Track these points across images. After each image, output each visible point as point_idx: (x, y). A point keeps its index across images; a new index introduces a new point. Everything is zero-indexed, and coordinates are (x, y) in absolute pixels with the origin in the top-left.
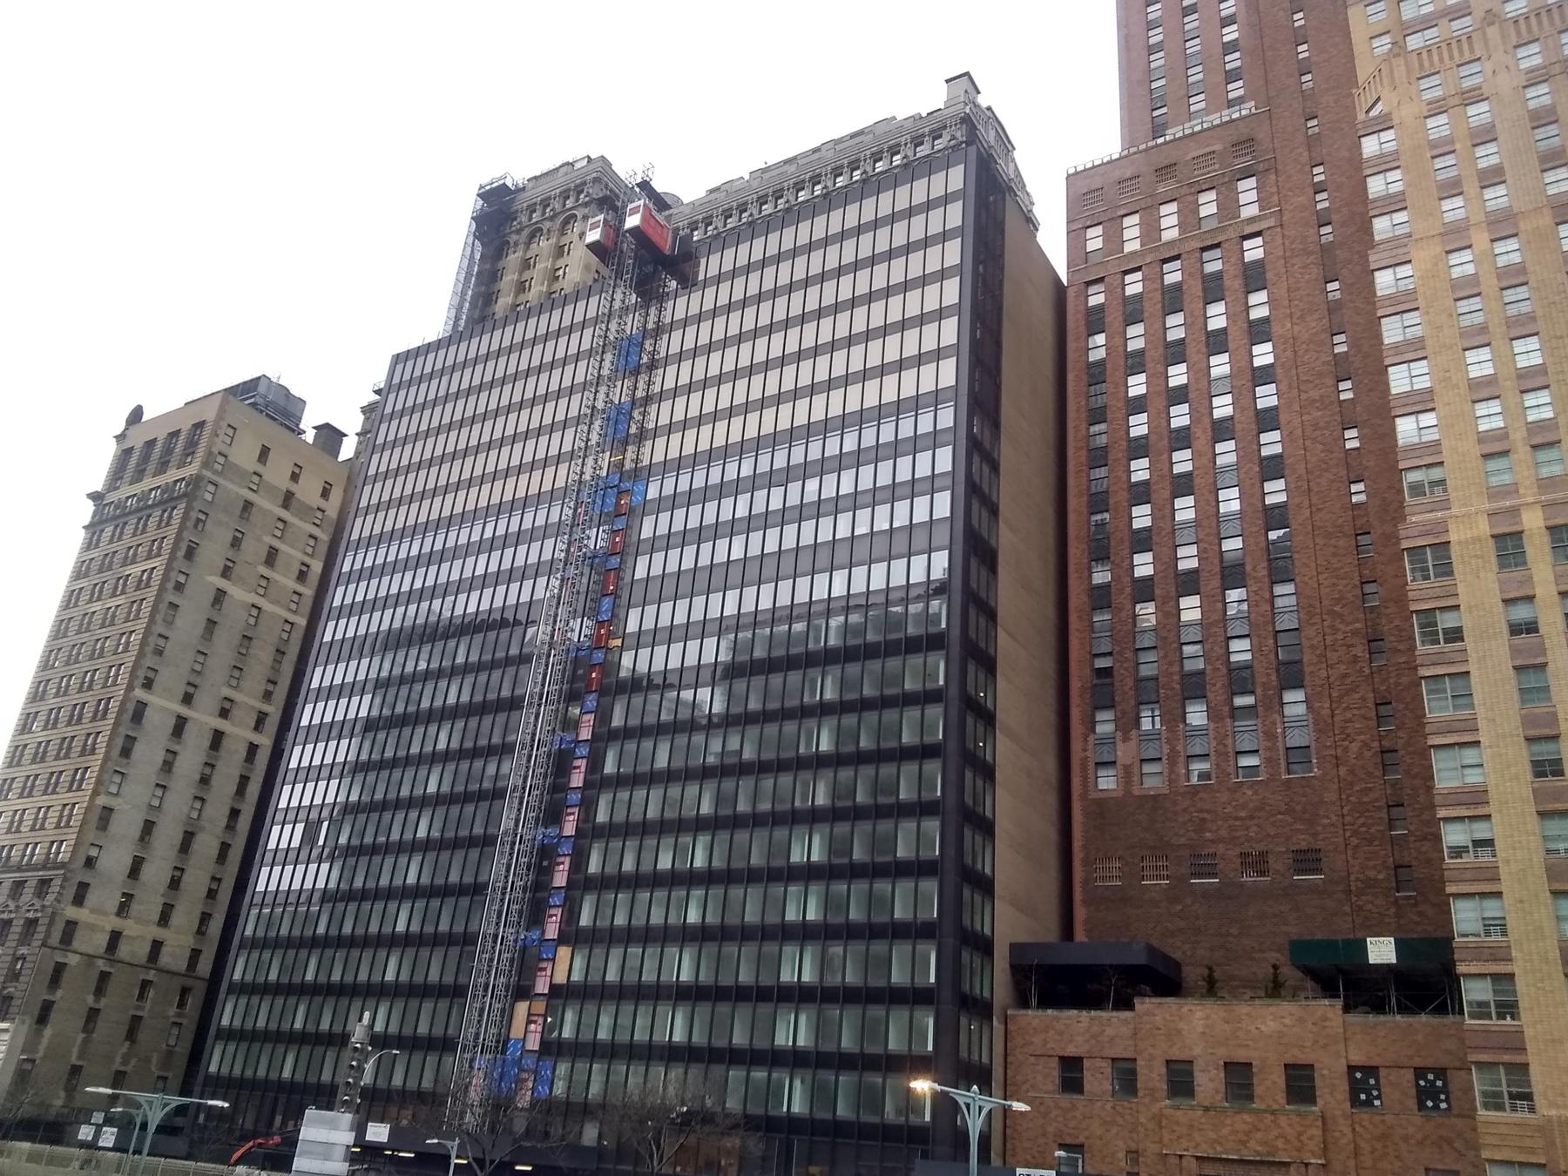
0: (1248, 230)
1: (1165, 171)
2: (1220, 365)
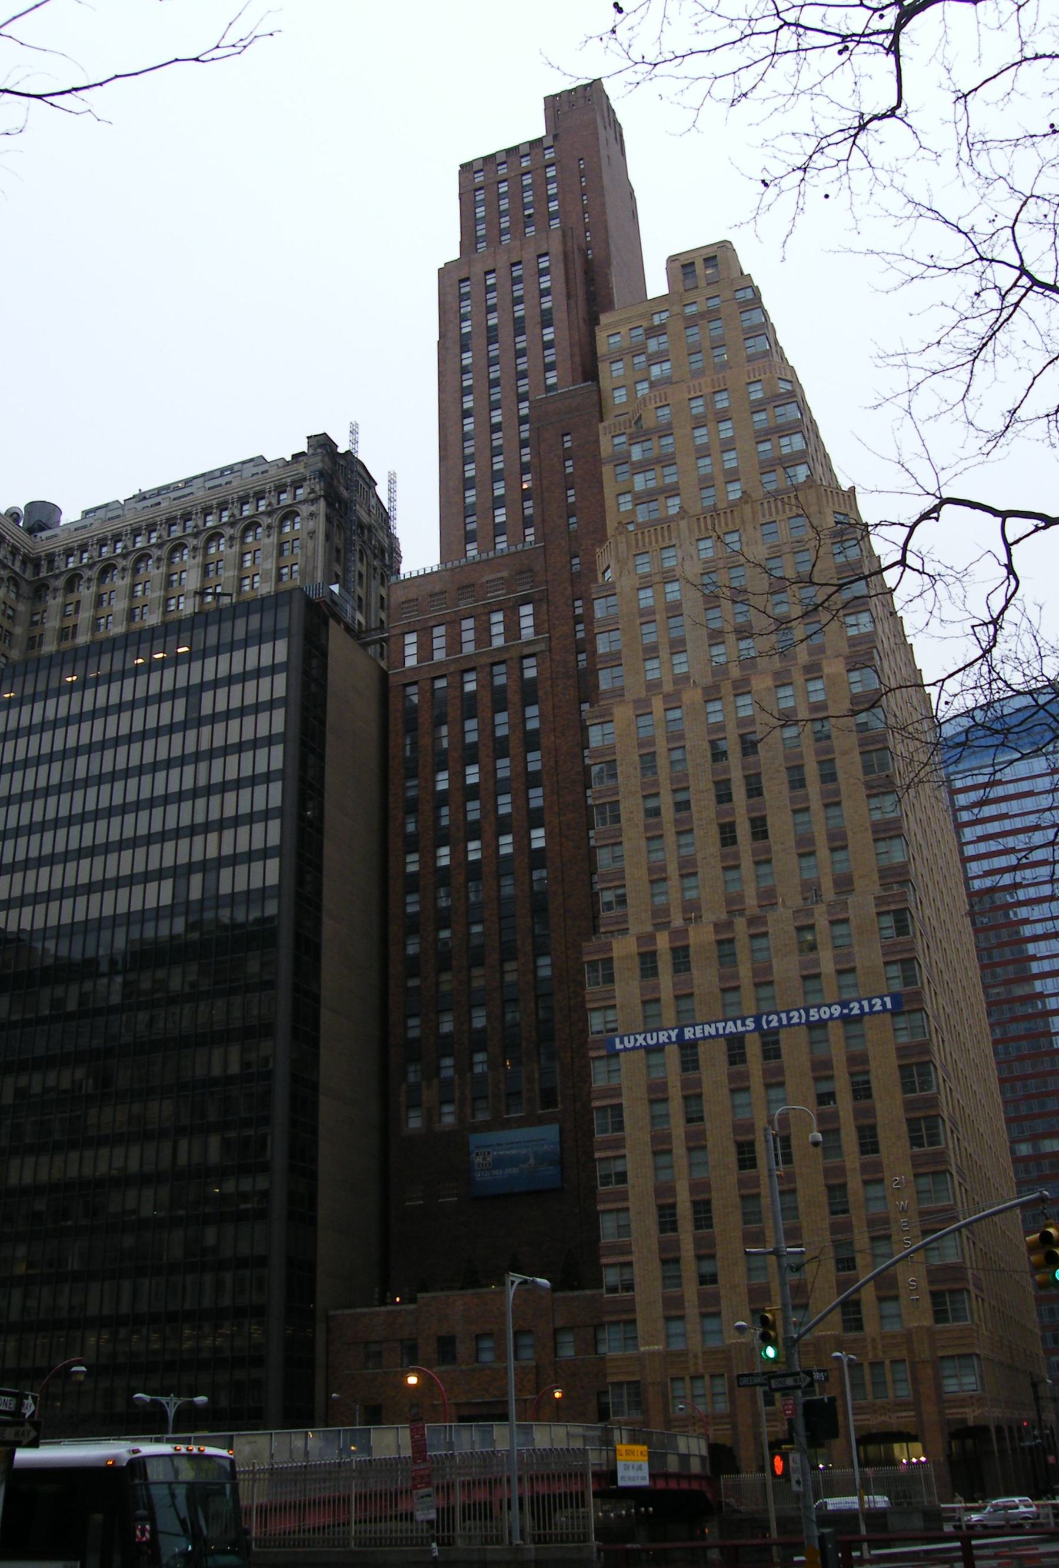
0: (526, 651)
1: (466, 589)
2: (504, 768)
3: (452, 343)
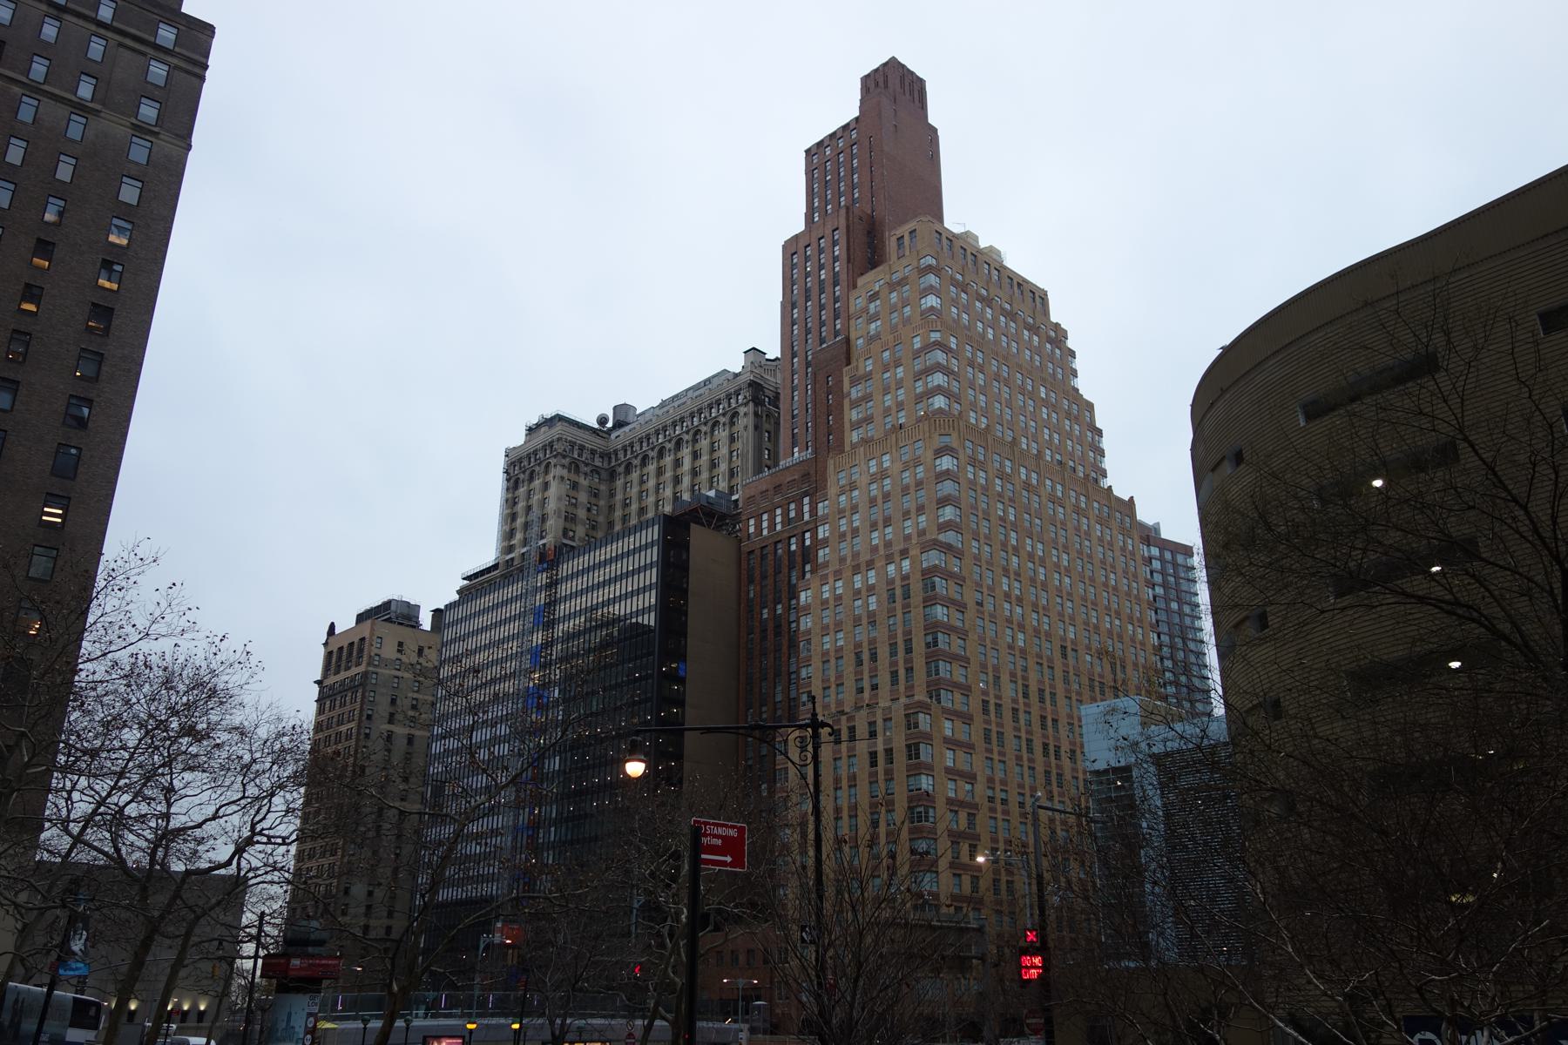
3: (788, 305)
